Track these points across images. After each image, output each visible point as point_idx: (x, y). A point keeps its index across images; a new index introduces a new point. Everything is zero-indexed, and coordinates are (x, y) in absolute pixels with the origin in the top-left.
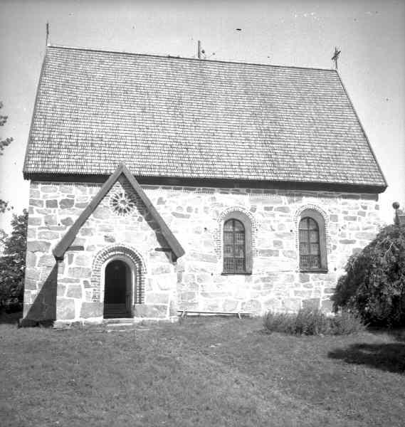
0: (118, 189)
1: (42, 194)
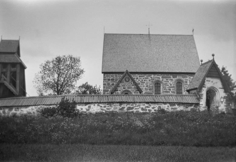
0: (127, 76)
1: (106, 77)
